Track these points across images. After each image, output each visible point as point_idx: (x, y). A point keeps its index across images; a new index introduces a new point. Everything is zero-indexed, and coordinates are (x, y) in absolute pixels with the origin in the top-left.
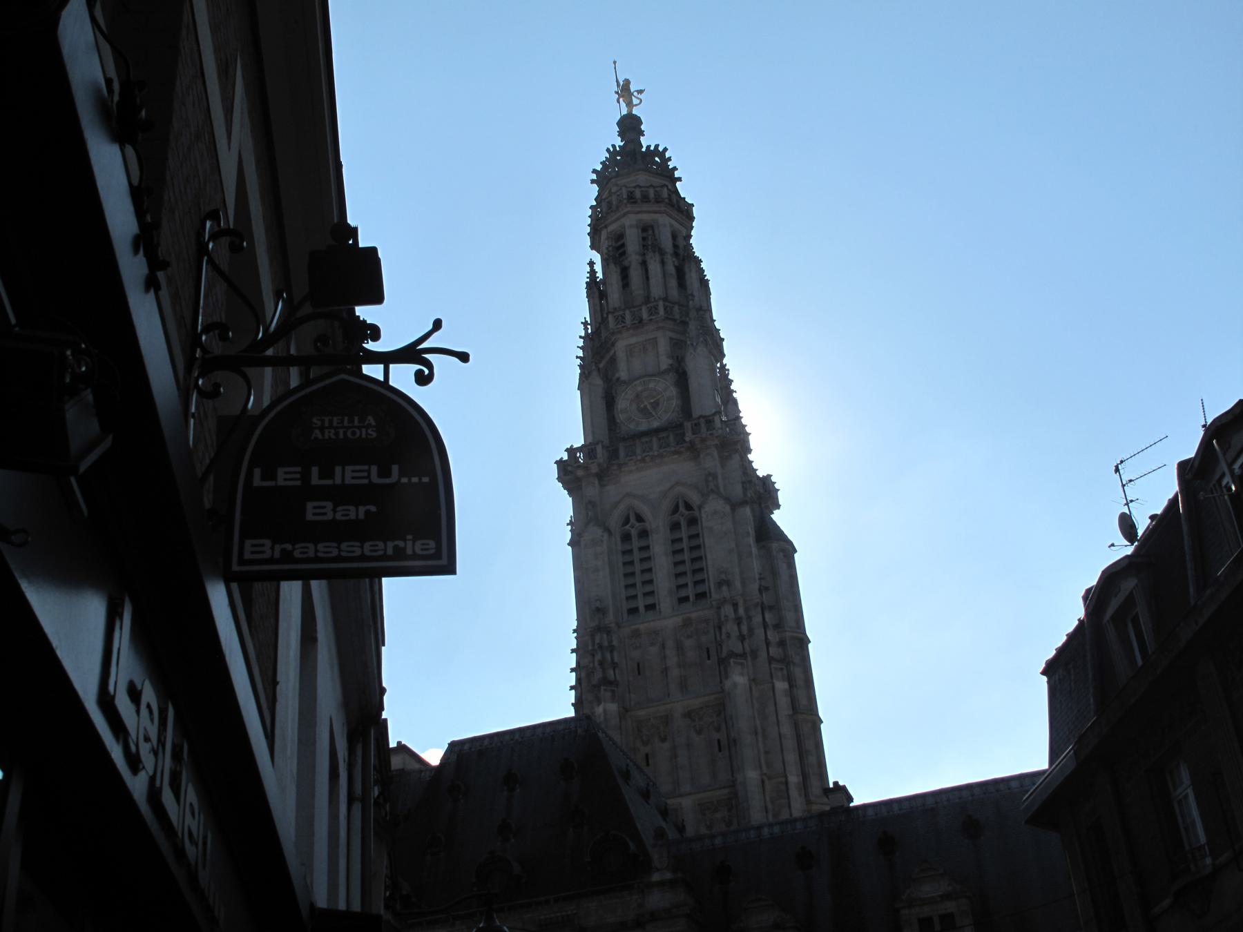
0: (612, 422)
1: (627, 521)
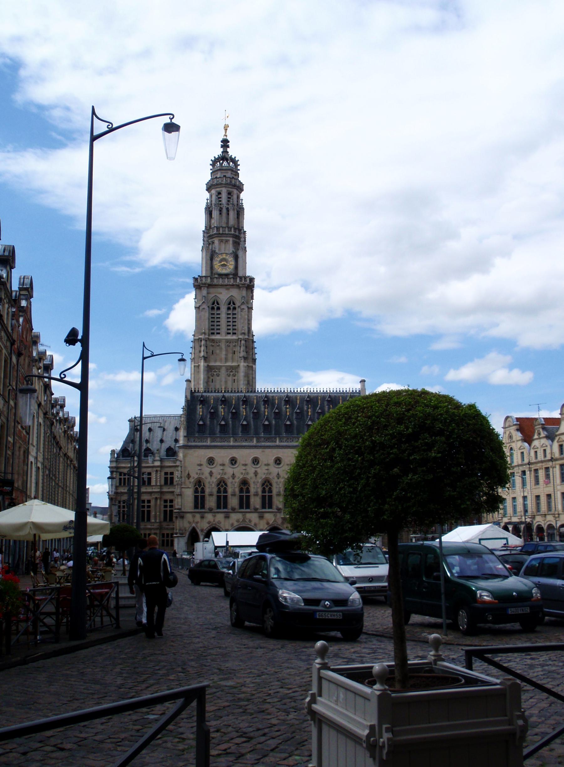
0: (212, 268)
1: (213, 303)
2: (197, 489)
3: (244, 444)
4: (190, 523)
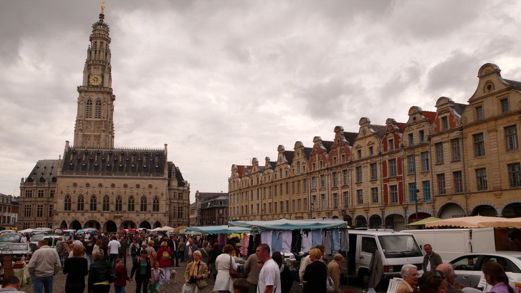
0: (89, 82)
1: (88, 101)
2: (66, 199)
3: (94, 176)
4: (61, 218)
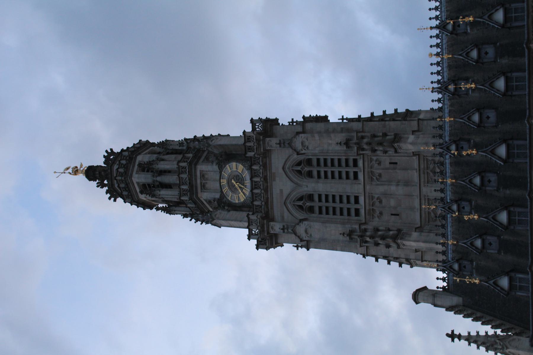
1: (301, 207)
